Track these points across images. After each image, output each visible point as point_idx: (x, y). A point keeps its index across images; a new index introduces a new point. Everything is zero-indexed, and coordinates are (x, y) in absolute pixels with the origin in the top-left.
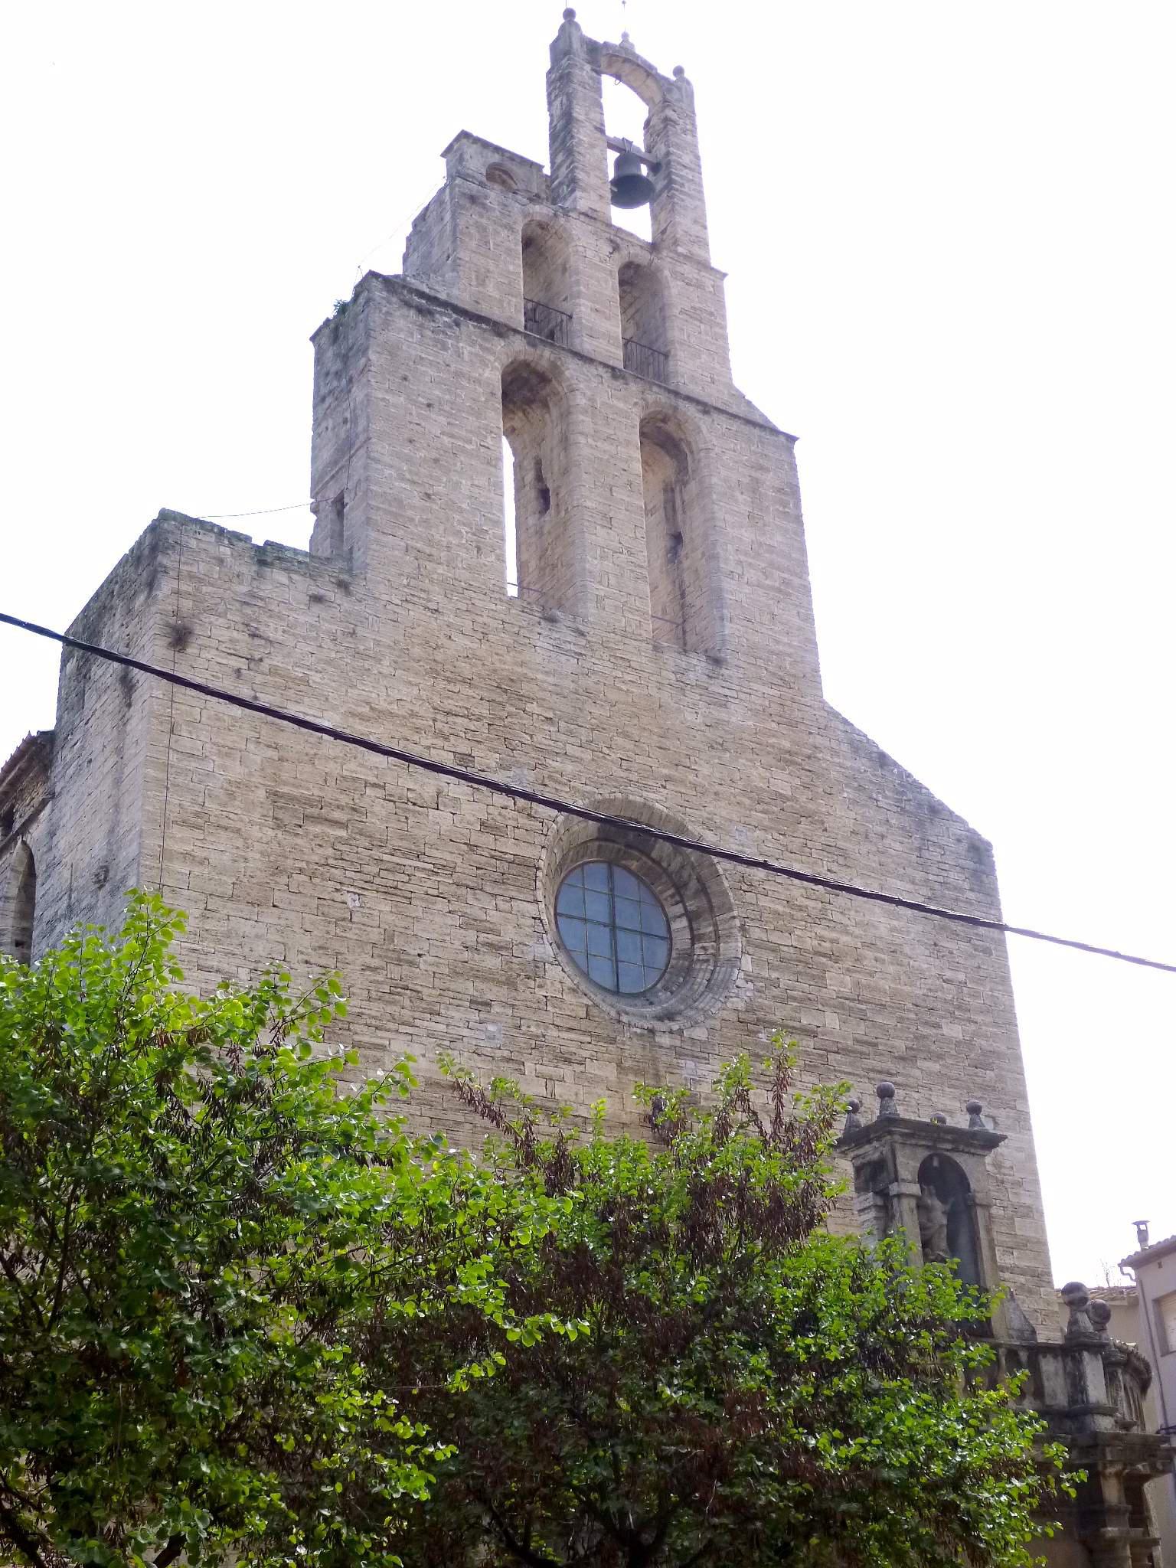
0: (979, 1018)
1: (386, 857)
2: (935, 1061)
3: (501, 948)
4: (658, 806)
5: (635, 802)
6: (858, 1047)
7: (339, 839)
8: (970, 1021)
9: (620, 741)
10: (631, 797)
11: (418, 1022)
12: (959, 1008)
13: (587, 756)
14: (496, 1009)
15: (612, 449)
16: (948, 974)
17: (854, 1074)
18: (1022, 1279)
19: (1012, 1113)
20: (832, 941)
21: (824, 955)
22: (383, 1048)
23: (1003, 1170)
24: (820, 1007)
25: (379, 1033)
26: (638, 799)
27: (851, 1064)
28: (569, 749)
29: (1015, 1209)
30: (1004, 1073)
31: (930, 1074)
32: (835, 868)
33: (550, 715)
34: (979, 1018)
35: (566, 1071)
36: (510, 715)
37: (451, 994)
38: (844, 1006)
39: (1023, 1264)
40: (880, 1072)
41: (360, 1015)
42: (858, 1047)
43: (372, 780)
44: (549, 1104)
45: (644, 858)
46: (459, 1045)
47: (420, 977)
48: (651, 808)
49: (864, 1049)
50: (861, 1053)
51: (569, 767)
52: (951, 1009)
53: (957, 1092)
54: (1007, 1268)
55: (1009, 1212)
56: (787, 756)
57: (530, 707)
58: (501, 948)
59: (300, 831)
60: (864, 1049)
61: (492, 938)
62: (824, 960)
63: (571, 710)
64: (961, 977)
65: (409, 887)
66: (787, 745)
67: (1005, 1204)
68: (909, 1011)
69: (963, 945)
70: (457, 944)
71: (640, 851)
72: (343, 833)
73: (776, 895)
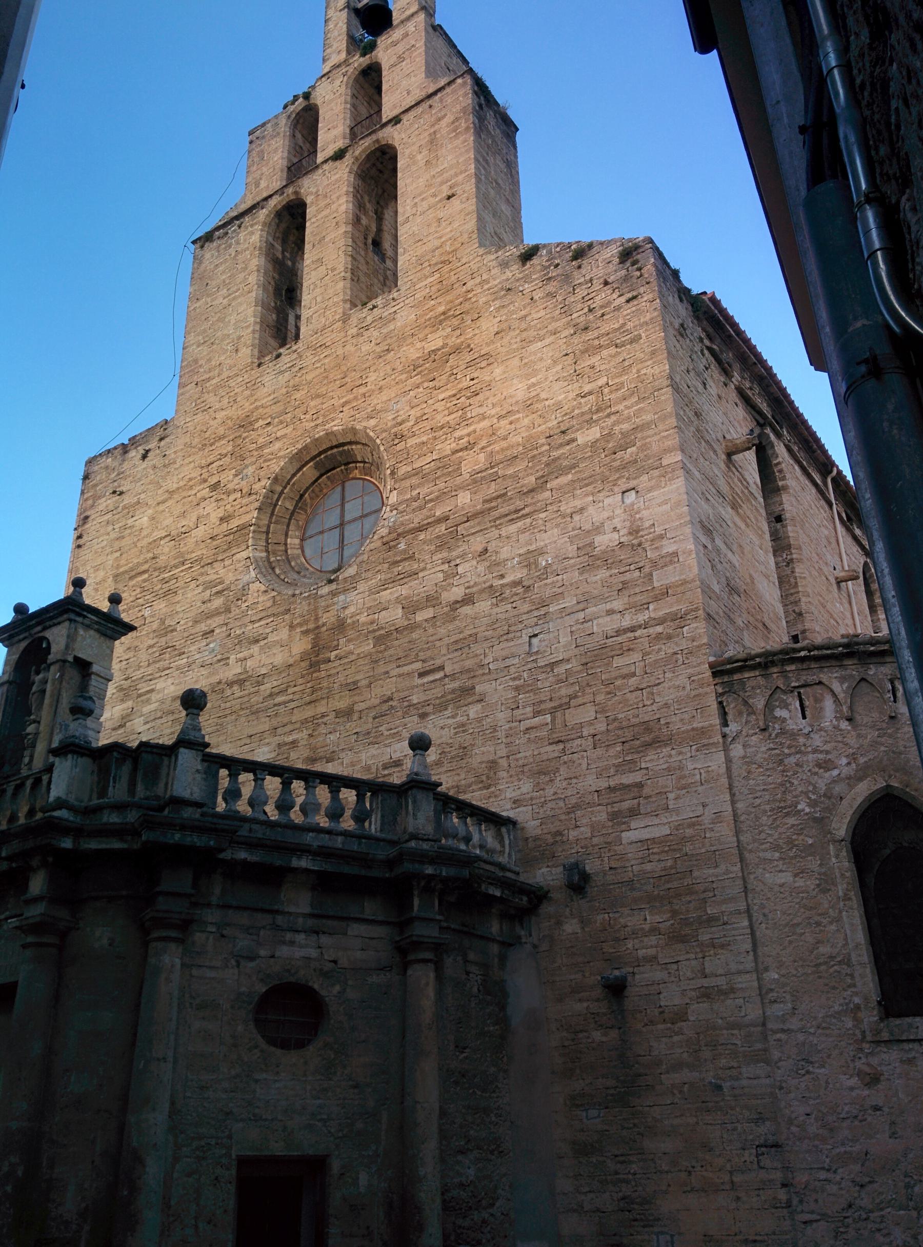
0: (620, 407)
1: (166, 575)
2: (567, 474)
3: (223, 591)
4: (335, 428)
5: (320, 437)
6: (487, 506)
7: (145, 581)
8: (609, 416)
9: (312, 403)
10: (317, 436)
11: (172, 665)
12: (598, 411)
13: (290, 429)
14: (217, 631)
15: (328, 211)
16: (587, 388)
17: (481, 530)
18: (659, 629)
19: (656, 473)
20: (469, 435)
21: (461, 450)
22: (152, 691)
23: (641, 533)
24: (454, 494)
25: (152, 683)
26: (322, 434)
27: (479, 524)
28: (279, 434)
29: (654, 564)
30: (648, 440)
31: (560, 488)
32: (475, 375)
33: (269, 420)
34: (620, 407)
35: (255, 649)
36: (244, 439)
37: (192, 637)
38: (476, 481)
39: (660, 613)
40: (507, 515)
41: (142, 677)
42: (487, 506)
43: (163, 535)
44: (242, 677)
45: (358, 465)
46: (193, 666)
47: (176, 639)
48: (332, 432)
49: (493, 504)
50: (490, 509)
51: (278, 445)
52: (587, 417)
53: (590, 488)
54: (640, 626)
55: (647, 570)
56: (442, 317)
57: (257, 425)
58: (223, 591)
59: (126, 588)
60: (493, 504)
61: (219, 588)
62: (460, 454)
63: (282, 408)
64: (603, 381)
65: (177, 585)
66: (442, 309)
67: (641, 565)
68: (543, 445)
69: (605, 353)
70: (199, 604)
71: (354, 462)
72: (146, 576)
73: (422, 430)
